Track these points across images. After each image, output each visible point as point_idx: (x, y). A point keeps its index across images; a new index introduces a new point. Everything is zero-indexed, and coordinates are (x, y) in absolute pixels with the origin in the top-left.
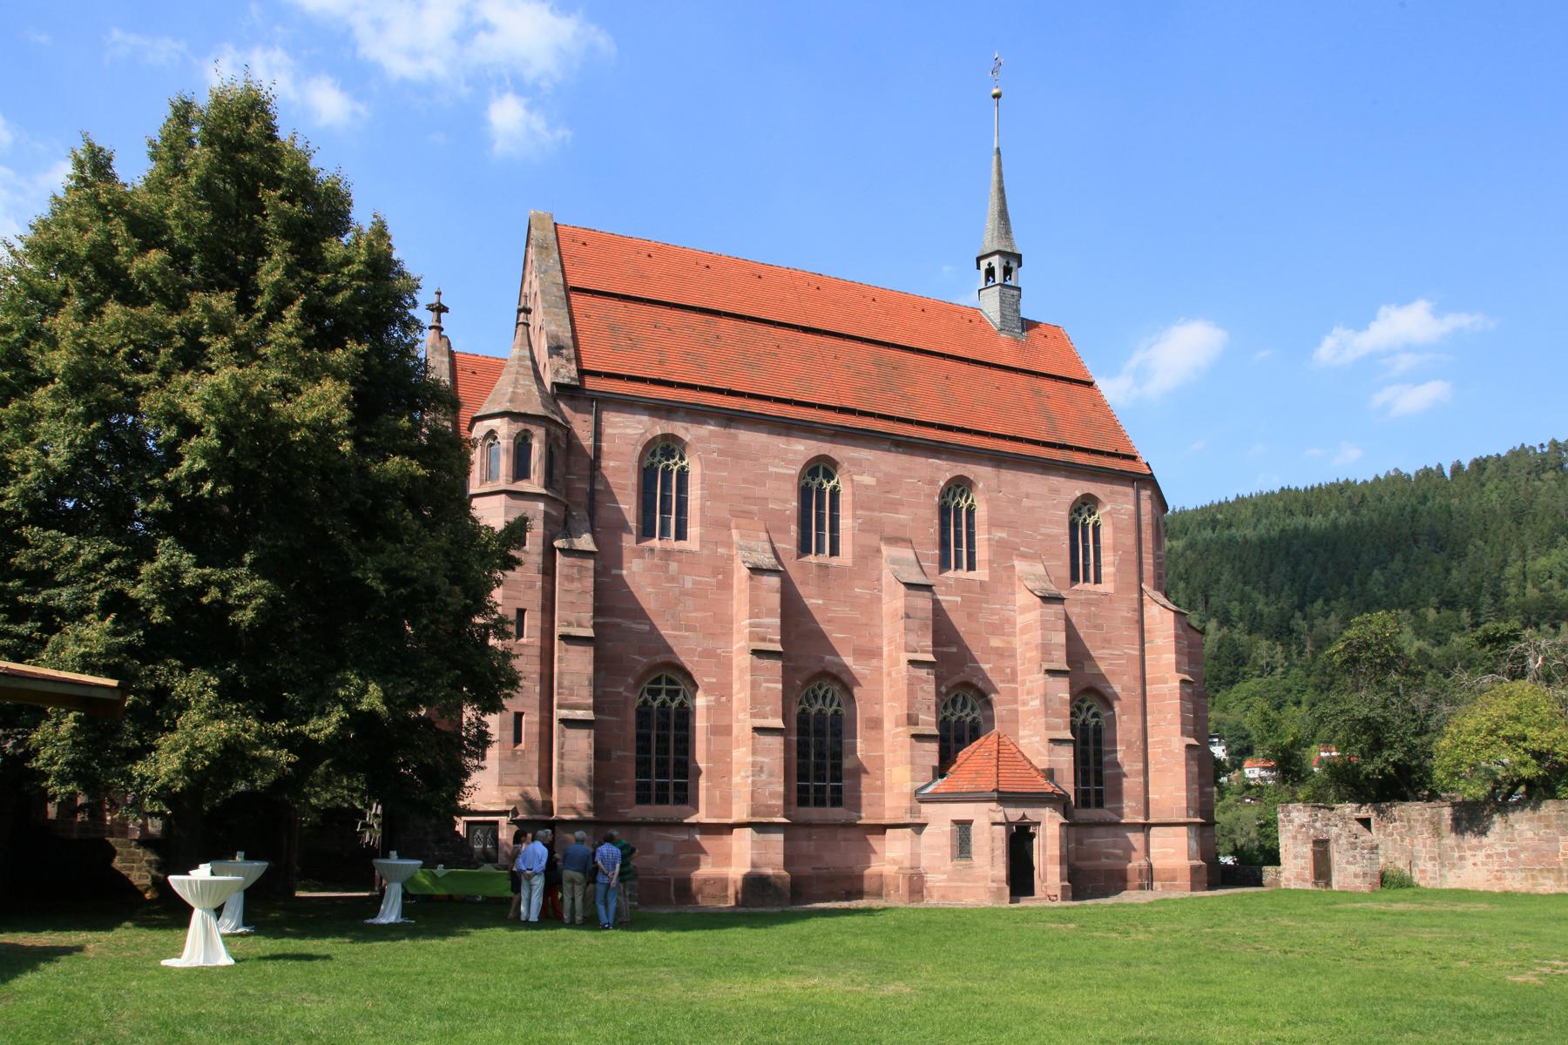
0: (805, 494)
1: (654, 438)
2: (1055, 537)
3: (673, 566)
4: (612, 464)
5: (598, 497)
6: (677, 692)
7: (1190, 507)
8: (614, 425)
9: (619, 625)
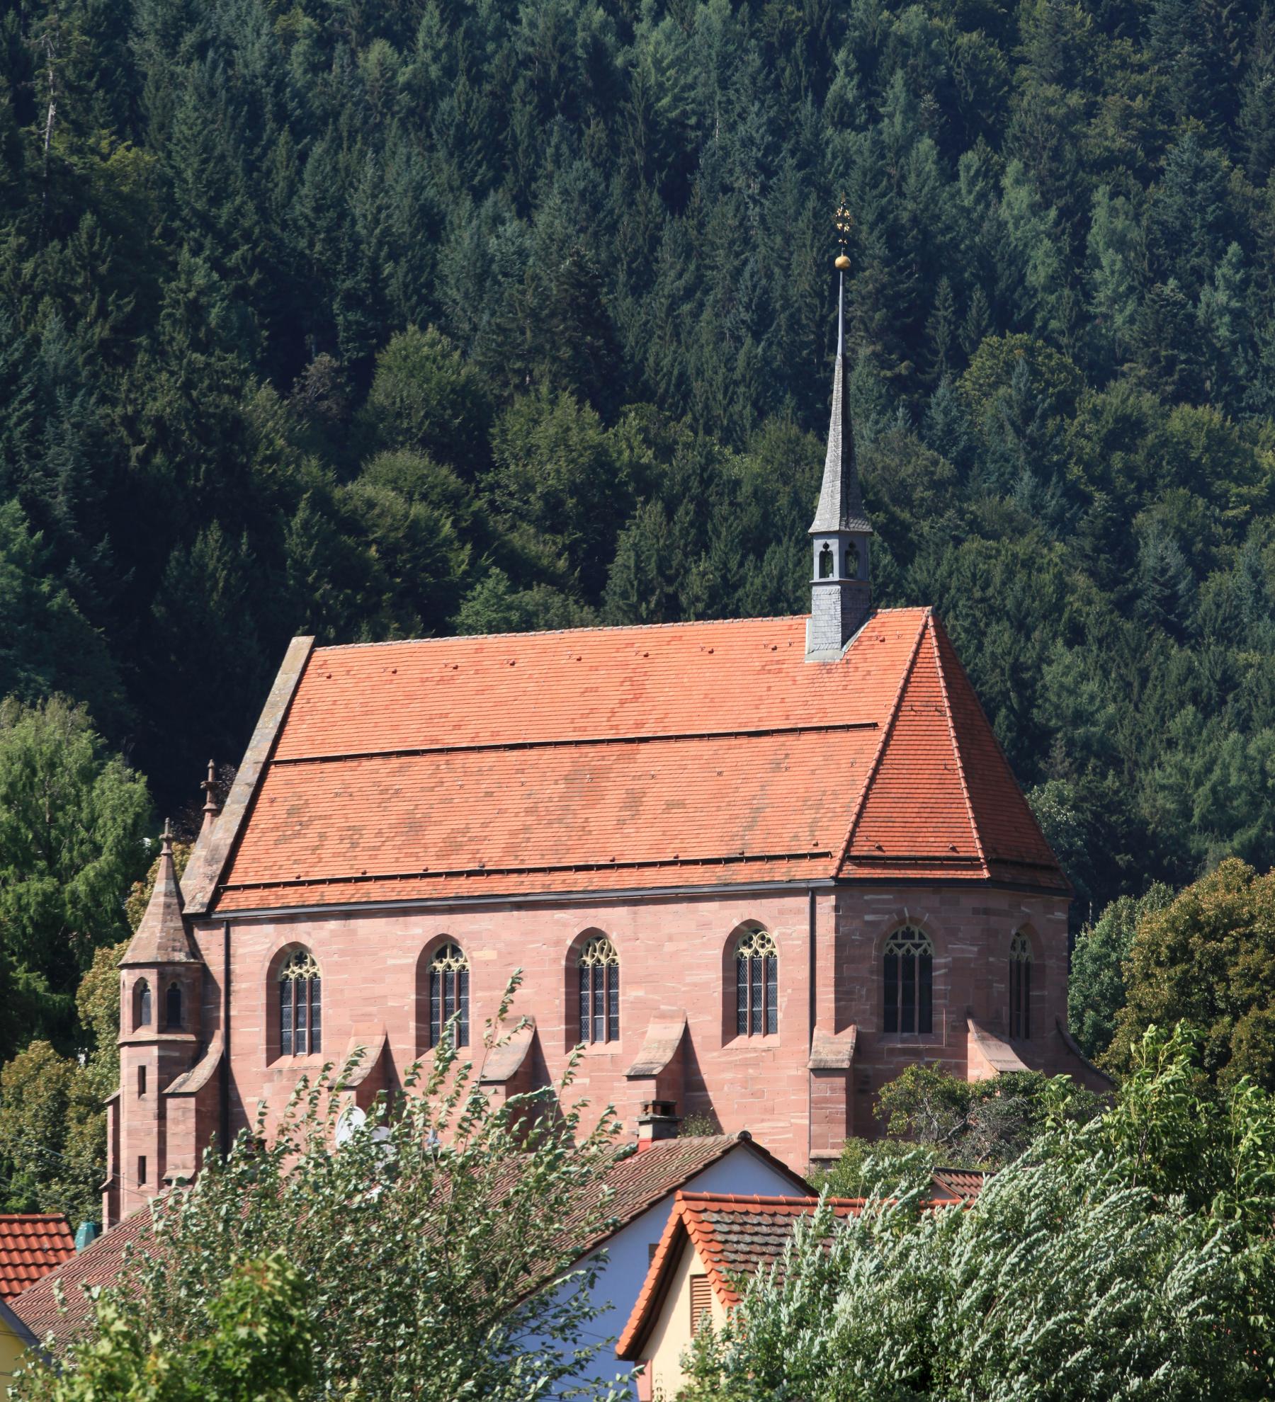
0: (426, 979)
1: (282, 950)
4: (244, 986)
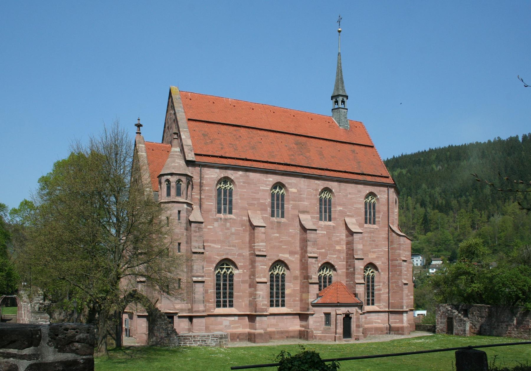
2: (360, 209)
3: (228, 224)
5: (202, 200)
6: (229, 268)
7: (409, 153)
8: (207, 174)
9: (210, 246)
